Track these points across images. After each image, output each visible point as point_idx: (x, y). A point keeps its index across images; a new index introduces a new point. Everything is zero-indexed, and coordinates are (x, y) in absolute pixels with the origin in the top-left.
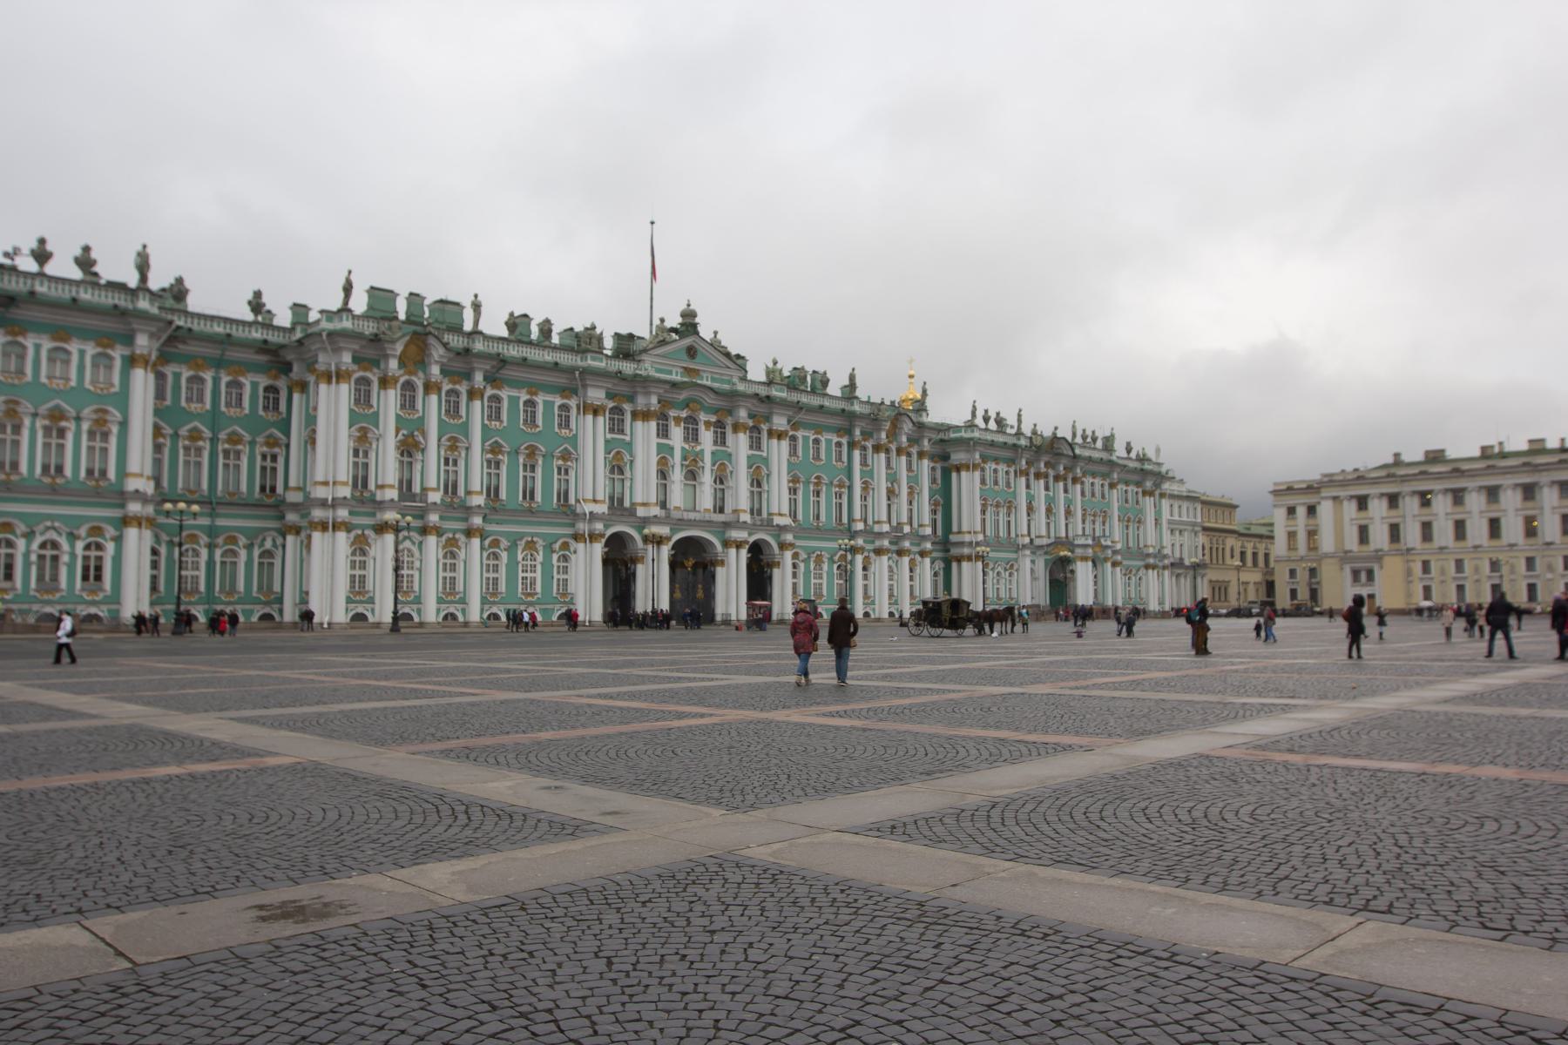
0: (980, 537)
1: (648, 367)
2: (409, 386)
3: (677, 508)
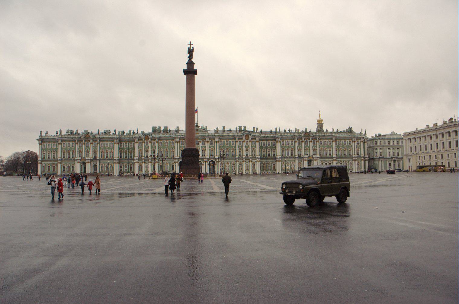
0: (280, 157)
2: (147, 142)
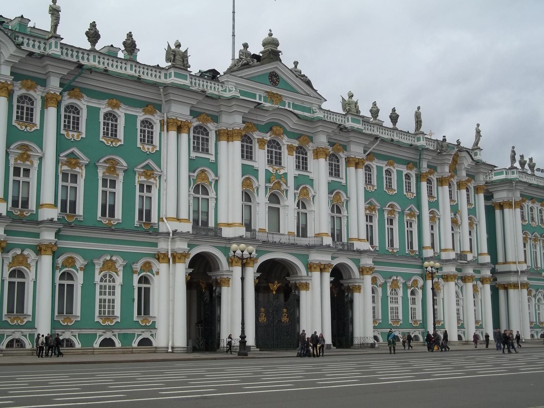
0: (524, 267)
1: (230, 90)
3: (262, 230)
